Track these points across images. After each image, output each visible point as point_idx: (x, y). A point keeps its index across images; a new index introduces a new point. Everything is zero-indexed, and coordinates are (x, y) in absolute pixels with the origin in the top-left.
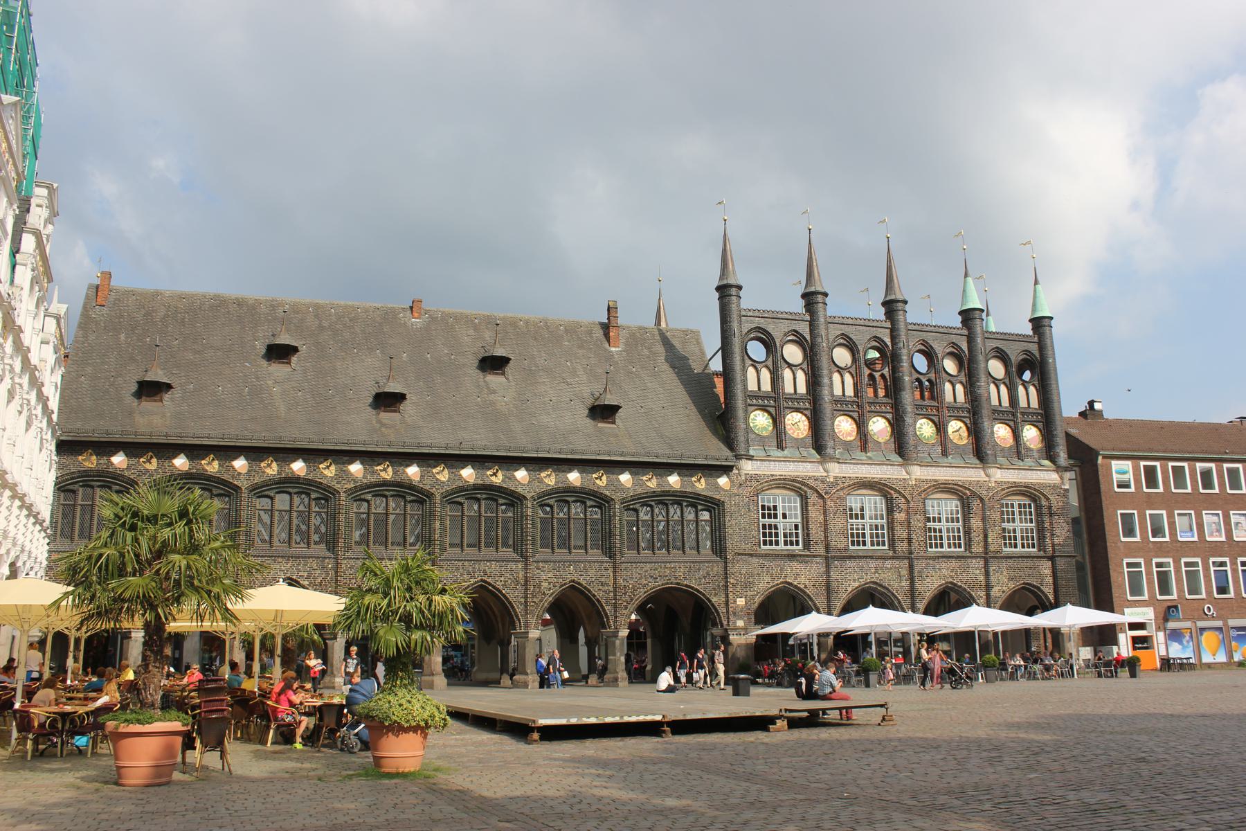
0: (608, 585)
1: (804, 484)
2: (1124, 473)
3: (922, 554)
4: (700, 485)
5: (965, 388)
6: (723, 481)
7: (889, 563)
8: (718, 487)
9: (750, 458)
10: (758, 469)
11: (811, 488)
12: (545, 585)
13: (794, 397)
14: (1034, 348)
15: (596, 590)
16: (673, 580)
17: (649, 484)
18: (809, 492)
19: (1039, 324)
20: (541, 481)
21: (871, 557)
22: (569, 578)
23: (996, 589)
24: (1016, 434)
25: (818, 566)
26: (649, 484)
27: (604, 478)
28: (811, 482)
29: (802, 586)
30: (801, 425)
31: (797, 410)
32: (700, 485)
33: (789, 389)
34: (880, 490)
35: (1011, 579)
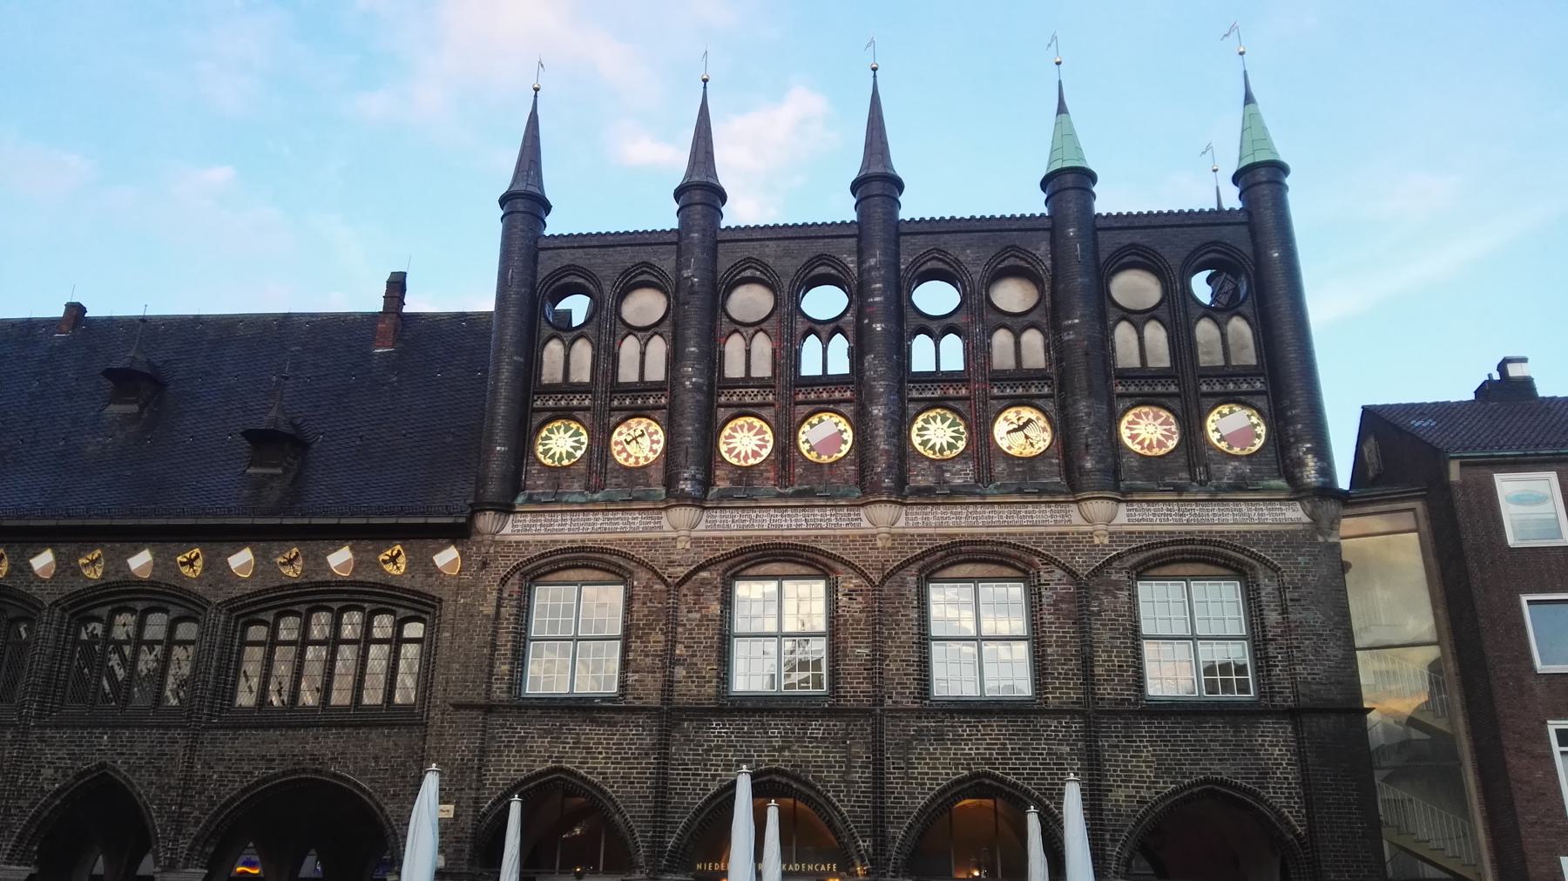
0: (170, 775)
1: (625, 556)
2: (1540, 500)
3: (907, 703)
4: (396, 564)
5: (1046, 336)
6: (447, 557)
7: (817, 728)
8: (432, 571)
9: (506, 509)
10: (526, 529)
11: (641, 563)
12: (48, 772)
13: (643, 387)
14: (1238, 238)
15: (143, 786)
16: (308, 764)
17: (285, 570)
18: (643, 576)
19: (1262, 180)
20: (77, 572)
21: (772, 712)
22: (97, 758)
23: (1120, 794)
24: (1191, 428)
25: (639, 735)
26: (285, 570)
27: (199, 563)
28: (641, 553)
29: (596, 779)
30: (645, 441)
31: (638, 412)
32: (396, 564)
33: (628, 373)
34: (810, 563)
35: (1163, 769)
